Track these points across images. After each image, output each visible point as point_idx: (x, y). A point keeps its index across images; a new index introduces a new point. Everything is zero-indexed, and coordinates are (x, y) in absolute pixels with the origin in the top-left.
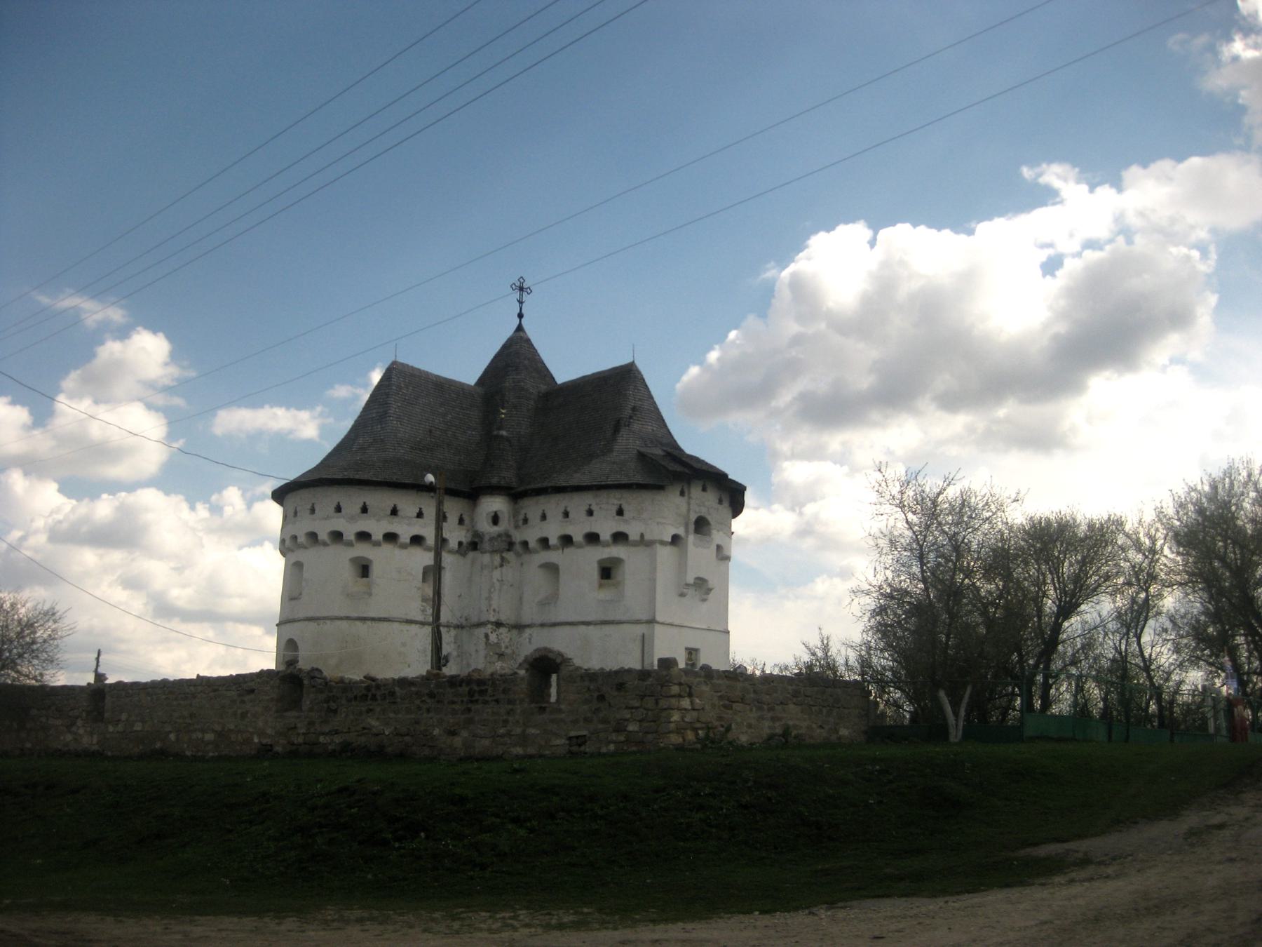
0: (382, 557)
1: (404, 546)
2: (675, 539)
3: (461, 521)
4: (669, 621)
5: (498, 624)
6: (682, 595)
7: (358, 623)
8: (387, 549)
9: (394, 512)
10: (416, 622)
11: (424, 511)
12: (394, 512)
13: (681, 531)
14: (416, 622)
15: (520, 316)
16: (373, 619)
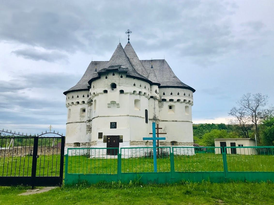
0: (73, 108)
1: (75, 105)
2: (106, 91)
3: (88, 96)
4: (104, 116)
5: (90, 121)
6: (108, 107)
7: (69, 124)
8: (73, 106)
9: (73, 97)
10: (78, 122)
11: (79, 96)
12: (73, 97)
13: (106, 89)
14: (78, 122)
15: (129, 39)
16: (70, 123)
